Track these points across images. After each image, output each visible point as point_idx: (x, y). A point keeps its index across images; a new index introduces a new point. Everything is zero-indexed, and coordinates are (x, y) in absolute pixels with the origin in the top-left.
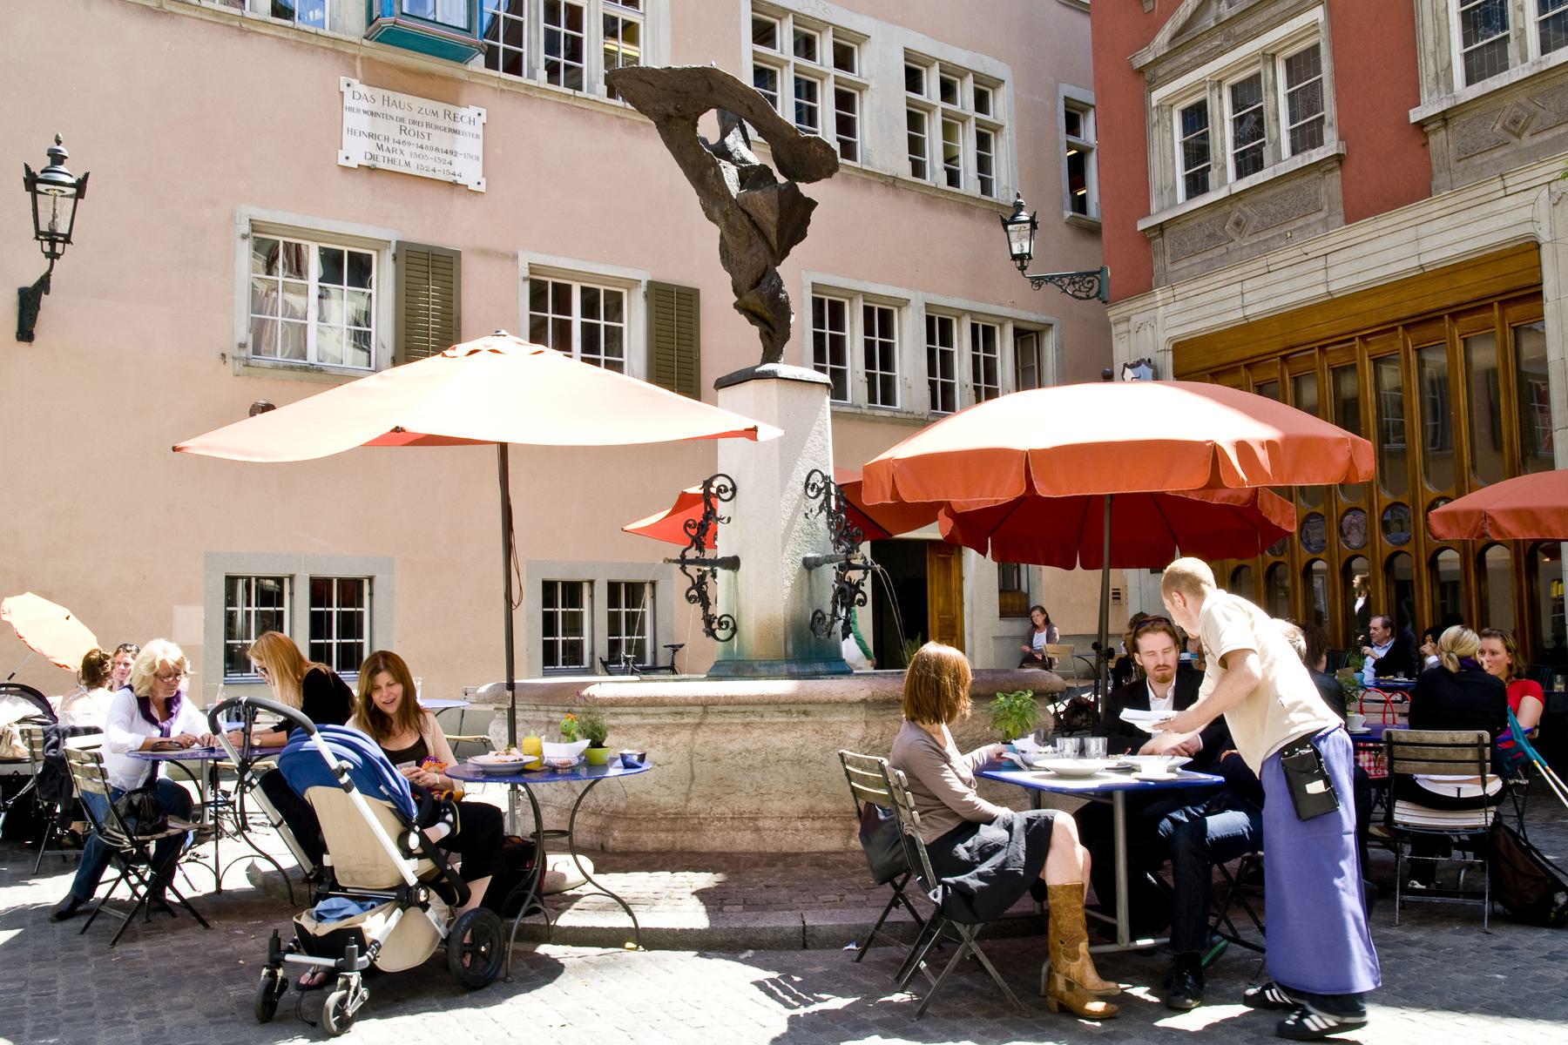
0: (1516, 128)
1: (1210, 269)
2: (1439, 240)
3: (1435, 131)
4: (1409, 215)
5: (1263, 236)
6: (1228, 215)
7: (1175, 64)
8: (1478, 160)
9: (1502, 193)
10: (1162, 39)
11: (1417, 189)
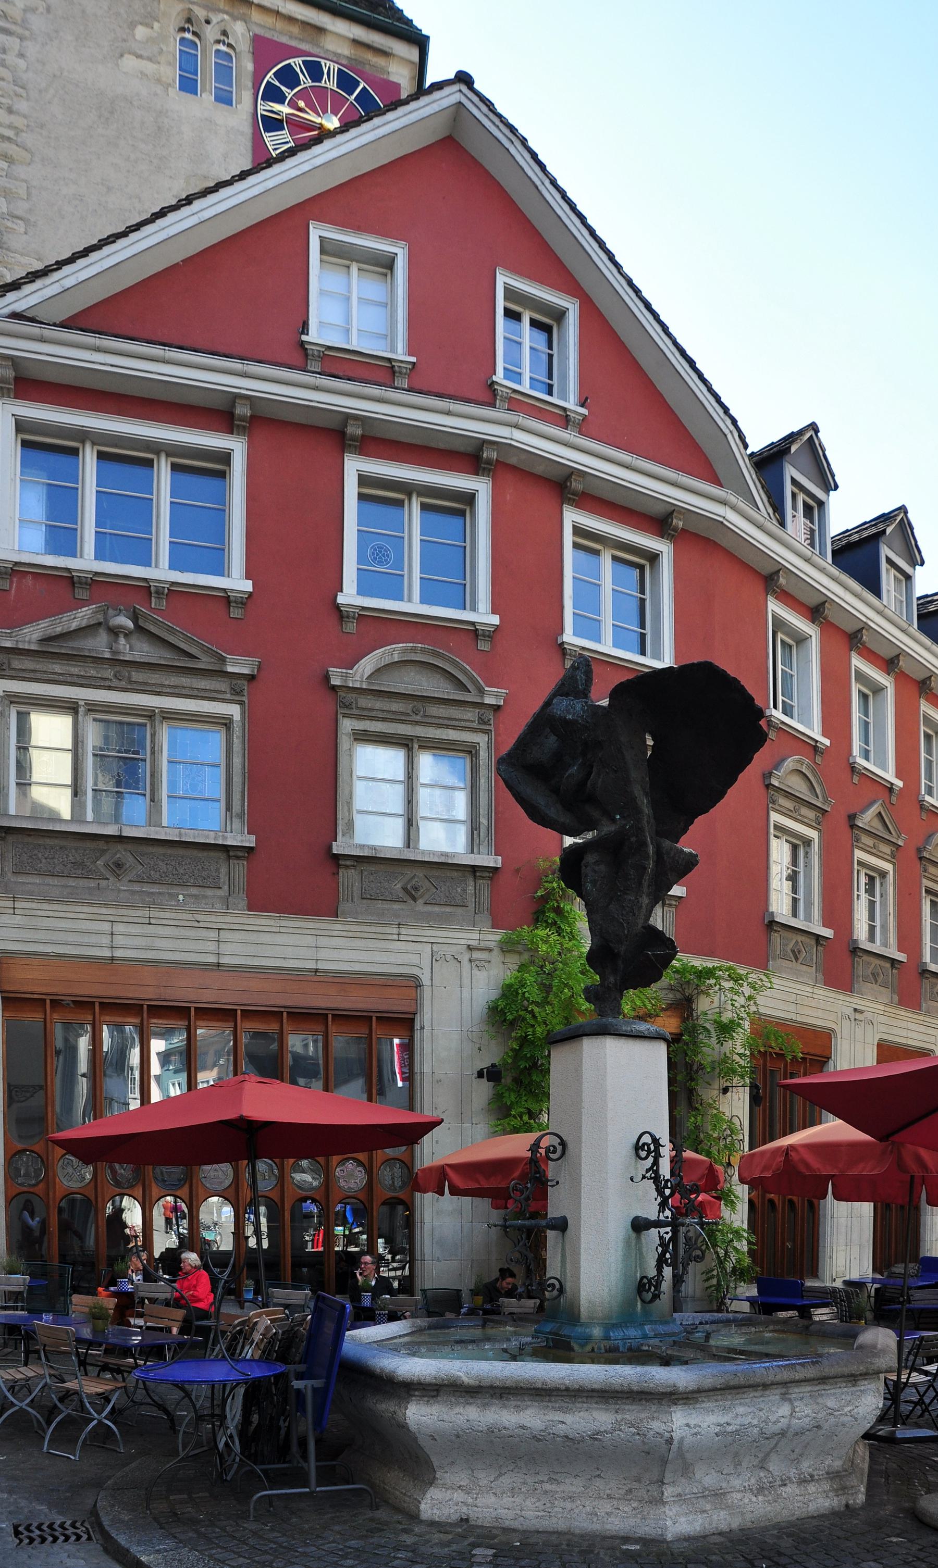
0: (411, 894)
1: (71, 898)
2: (333, 955)
3: (347, 867)
4: (312, 925)
5: (146, 888)
6: (103, 852)
7: (39, 667)
8: (379, 905)
9: (396, 937)
10: (31, 635)
11: (328, 908)
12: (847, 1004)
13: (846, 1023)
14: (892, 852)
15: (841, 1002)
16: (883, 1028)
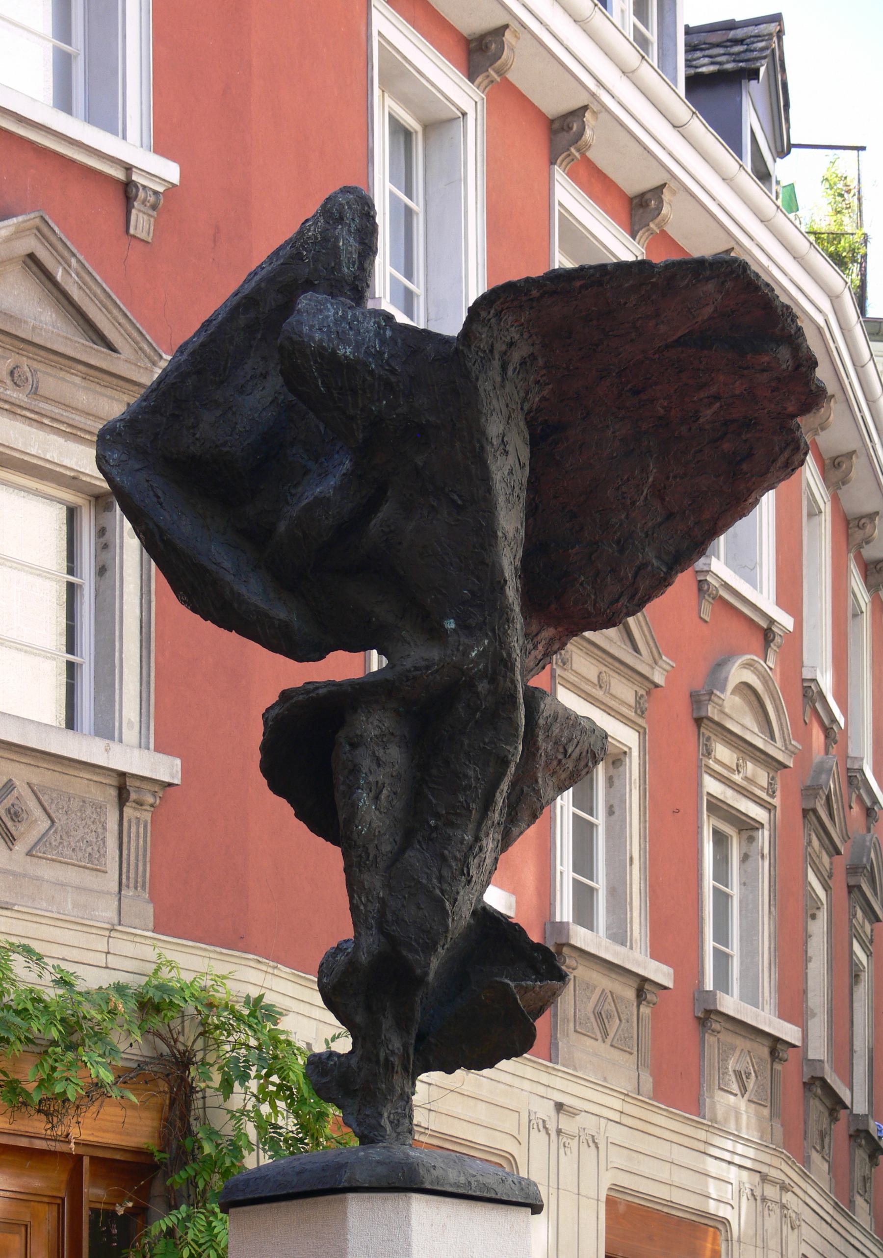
12: (541, 1090)
13: (539, 1139)
14: (638, 698)
15: (527, 1085)
16: (618, 1158)
